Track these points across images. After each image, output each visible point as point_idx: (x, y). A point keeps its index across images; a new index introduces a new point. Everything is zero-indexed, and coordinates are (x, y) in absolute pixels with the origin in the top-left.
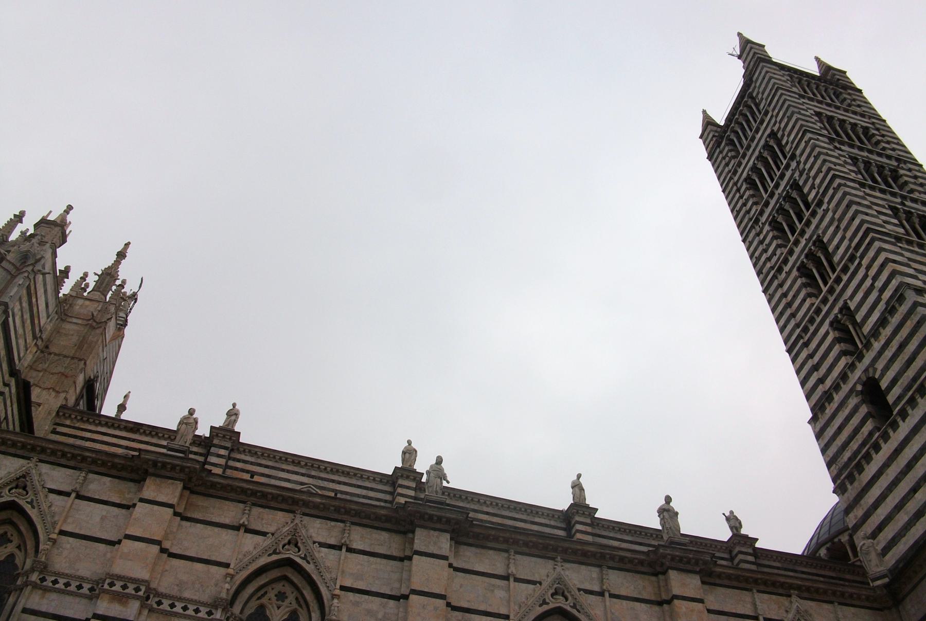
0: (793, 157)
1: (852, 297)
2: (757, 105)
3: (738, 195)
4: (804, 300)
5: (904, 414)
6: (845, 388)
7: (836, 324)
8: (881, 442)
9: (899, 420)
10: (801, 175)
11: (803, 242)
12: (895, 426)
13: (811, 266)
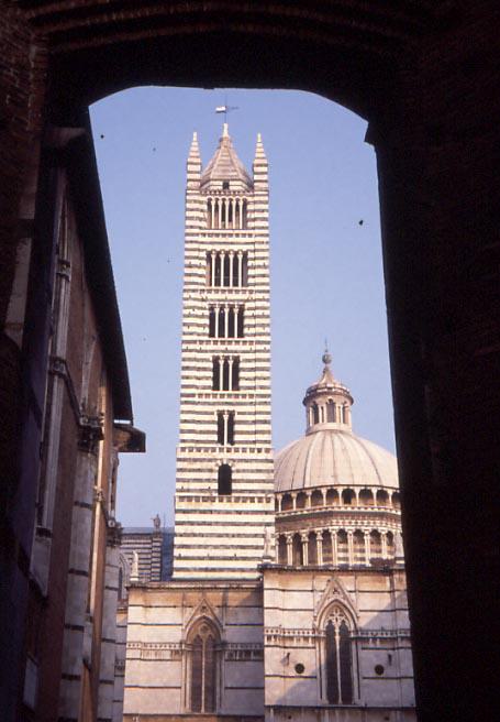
0: (251, 292)
1: (239, 413)
2: (246, 221)
3: (196, 254)
4: (207, 378)
5: (237, 500)
6: (209, 455)
7: (220, 414)
8: (217, 500)
9: (233, 500)
10: (249, 309)
11: (223, 347)
12: (229, 501)
13: (222, 362)
